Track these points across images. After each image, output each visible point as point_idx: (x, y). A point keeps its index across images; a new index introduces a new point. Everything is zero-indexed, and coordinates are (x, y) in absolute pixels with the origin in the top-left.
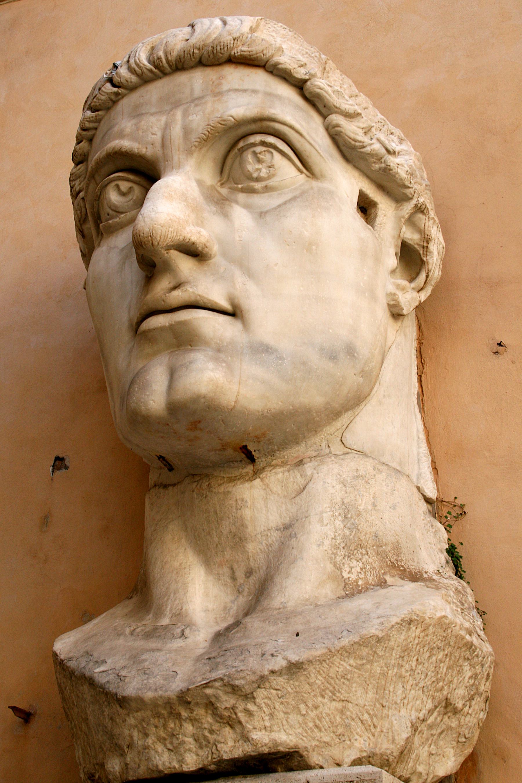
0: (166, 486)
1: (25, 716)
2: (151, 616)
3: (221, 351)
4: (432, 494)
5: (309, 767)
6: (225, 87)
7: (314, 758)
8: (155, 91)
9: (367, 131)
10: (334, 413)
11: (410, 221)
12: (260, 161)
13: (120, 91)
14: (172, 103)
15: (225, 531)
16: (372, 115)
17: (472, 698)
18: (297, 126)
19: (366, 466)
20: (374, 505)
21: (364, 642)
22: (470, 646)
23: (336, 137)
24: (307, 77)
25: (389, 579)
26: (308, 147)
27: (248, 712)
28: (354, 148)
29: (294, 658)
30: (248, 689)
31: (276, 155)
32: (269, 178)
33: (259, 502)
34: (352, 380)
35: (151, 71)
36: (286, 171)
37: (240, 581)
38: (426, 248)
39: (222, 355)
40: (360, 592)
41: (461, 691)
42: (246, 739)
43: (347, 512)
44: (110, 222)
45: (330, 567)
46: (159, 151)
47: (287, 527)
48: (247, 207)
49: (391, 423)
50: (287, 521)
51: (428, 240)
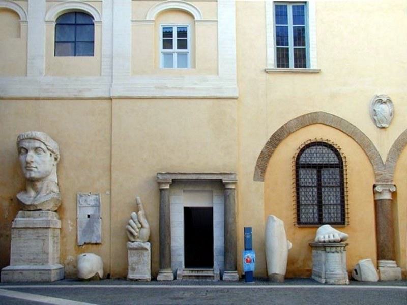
1: (12, 200)
3: (35, 172)
8: (27, 140)
14: (29, 142)
23: (47, 148)
33: (39, 185)
34: (48, 173)
49: (54, 177)
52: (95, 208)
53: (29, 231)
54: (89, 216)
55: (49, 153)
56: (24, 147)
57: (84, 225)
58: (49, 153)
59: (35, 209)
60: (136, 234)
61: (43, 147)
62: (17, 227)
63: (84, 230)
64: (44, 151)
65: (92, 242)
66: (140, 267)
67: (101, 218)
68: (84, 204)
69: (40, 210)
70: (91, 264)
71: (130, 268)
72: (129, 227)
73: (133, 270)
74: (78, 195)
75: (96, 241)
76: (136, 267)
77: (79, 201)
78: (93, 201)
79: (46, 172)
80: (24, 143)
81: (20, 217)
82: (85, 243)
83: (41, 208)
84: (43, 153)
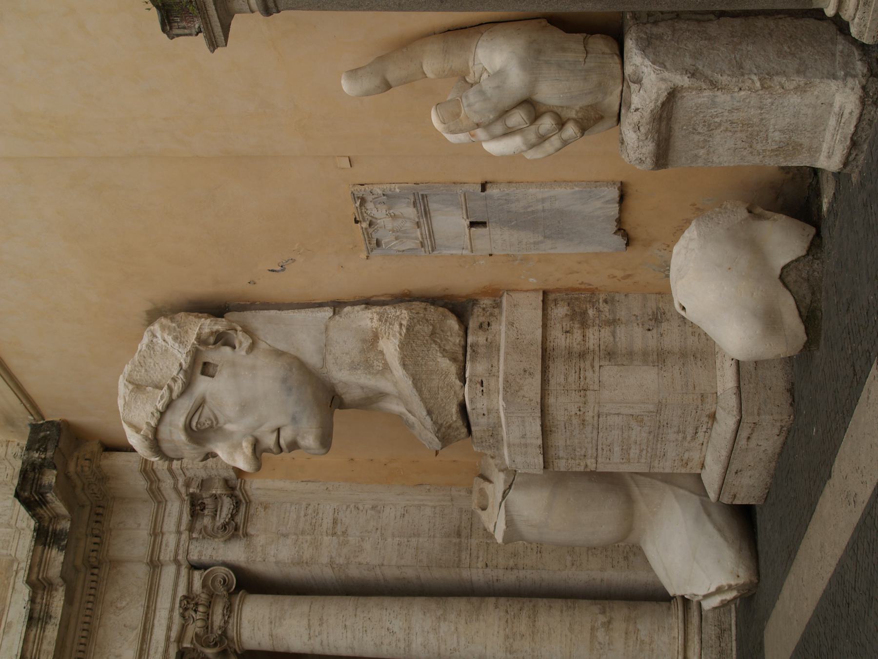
7: (461, 398)
17: (427, 320)
21: (415, 385)
23: (182, 393)
43: (353, 367)
51: (212, 333)
52: (433, 206)
55: (203, 385)
59: (460, 423)
61: (178, 418)
63: (545, 237)
64: (201, 404)
67: (484, 187)
69: (462, 407)
76: (777, 136)
79: (289, 389)
83: (454, 409)
84: (206, 412)
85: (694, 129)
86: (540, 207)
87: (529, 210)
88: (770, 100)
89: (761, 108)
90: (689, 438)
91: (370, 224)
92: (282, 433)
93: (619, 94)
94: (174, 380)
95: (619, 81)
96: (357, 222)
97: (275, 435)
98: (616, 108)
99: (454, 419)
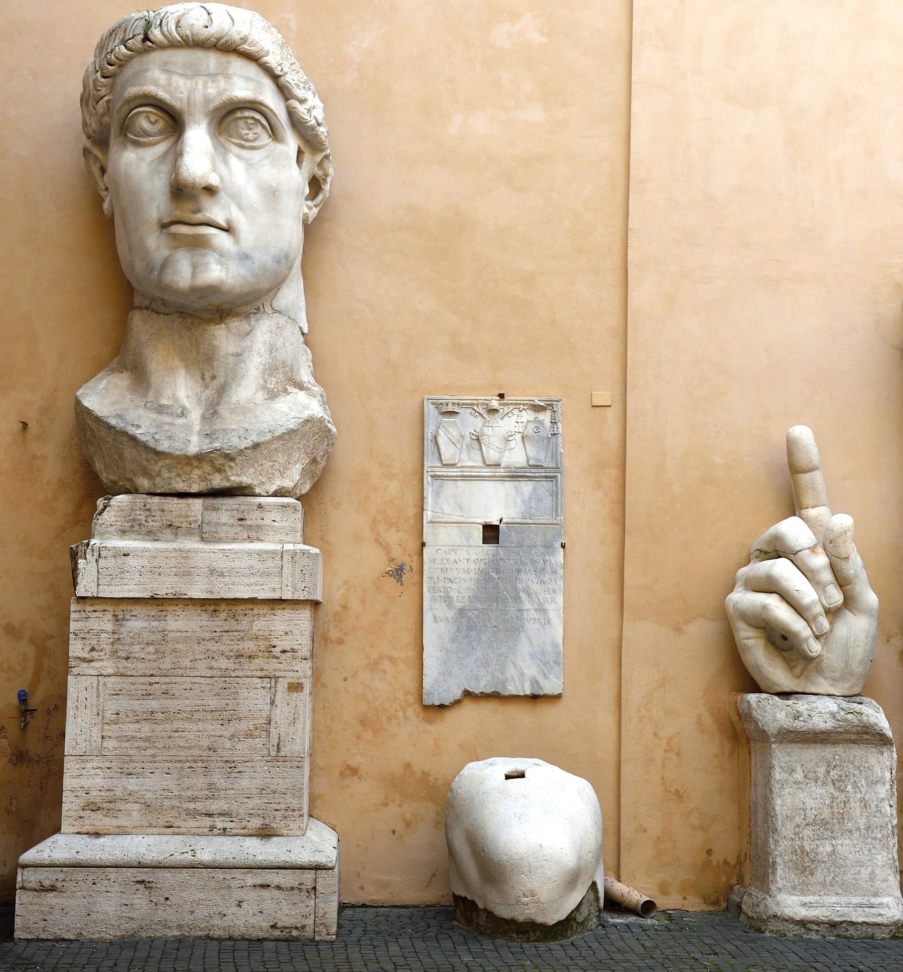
0: (158, 313)
2: (151, 394)
4: (306, 331)
5: (255, 495)
6: (231, 71)
8: (180, 57)
9: (309, 111)
10: (270, 290)
11: (320, 165)
12: (250, 129)
13: (154, 46)
15: (202, 352)
16: (314, 101)
18: (275, 110)
19: (282, 320)
20: (284, 344)
22: (330, 430)
23: (291, 114)
24: (281, 74)
25: (290, 389)
26: (278, 122)
27: (231, 467)
28: (302, 123)
29: (256, 440)
30: (232, 456)
31: (260, 127)
32: (254, 140)
33: (223, 338)
35: (179, 42)
36: (265, 139)
37: (208, 381)
38: (325, 180)
39: (223, 259)
40: (276, 396)
41: (321, 453)
42: (228, 480)
43: (272, 349)
44: (142, 140)
45: (262, 382)
46: (185, 109)
47: (238, 355)
48: (239, 157)
50: (239, 351)
51: (327, 176)
52: (527, 487)
53: (179, 623)
54: (491, 533)
56: (162, 94)
57: (463, 587)
58: (292, 143)
59: (218, 482)
60: (815, 648)
62: (106, 592)
63: (461, 611)
64: (274, 134)
65: (512, 689)
66: (845, 846)
67: (563, 546)
68: (471, 460)
70: (543, 822)
71: (782, 850)
72: (773, 603)
73: (806, 865)
74: (431, 411)
75: (535, 682)
77: (435, 439)
78: (516, 443)
80: (156, 74)
81: (123, 532)
82: (467, 694)
83: (245, 480)
85: (835, 767)
86: (527, 605)
87: (522, 594)
88: (879, 836)
89: (868, 828)
90: (192, 806)
91: (493, 411)
92: (223, 234)
93: (830, 693)
94: (309, 111)
95: (846, 693)
96: (501, 396)
97: (223, 224)
98: (814, 690)
99: (233, 478)
